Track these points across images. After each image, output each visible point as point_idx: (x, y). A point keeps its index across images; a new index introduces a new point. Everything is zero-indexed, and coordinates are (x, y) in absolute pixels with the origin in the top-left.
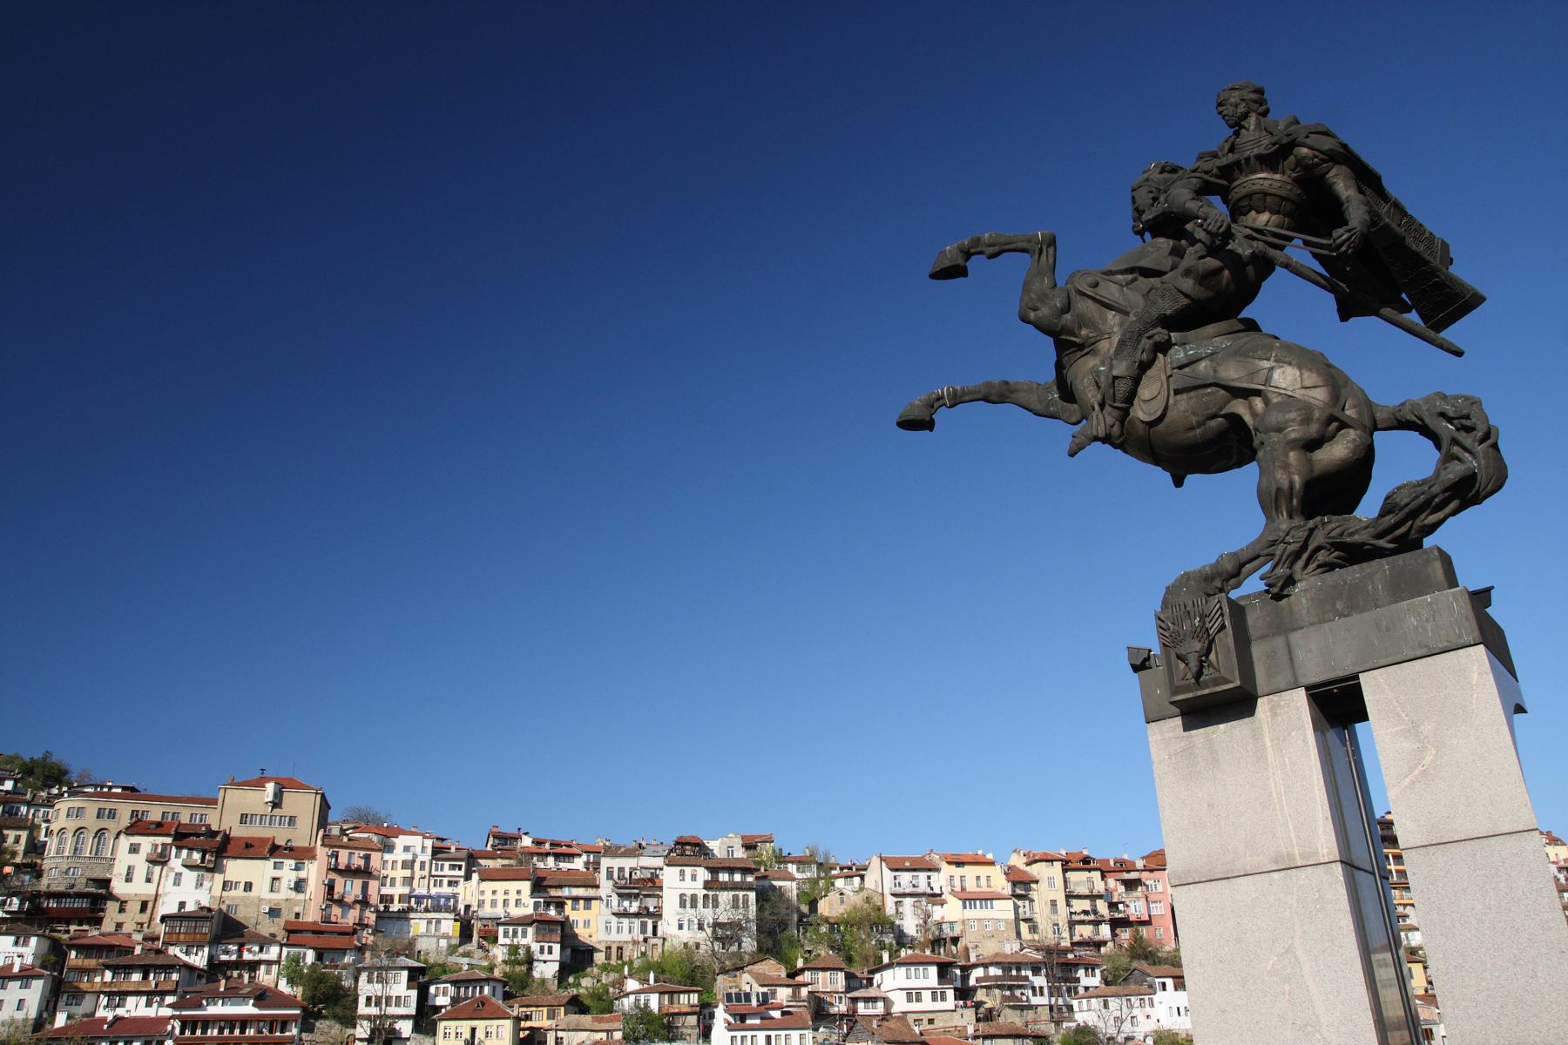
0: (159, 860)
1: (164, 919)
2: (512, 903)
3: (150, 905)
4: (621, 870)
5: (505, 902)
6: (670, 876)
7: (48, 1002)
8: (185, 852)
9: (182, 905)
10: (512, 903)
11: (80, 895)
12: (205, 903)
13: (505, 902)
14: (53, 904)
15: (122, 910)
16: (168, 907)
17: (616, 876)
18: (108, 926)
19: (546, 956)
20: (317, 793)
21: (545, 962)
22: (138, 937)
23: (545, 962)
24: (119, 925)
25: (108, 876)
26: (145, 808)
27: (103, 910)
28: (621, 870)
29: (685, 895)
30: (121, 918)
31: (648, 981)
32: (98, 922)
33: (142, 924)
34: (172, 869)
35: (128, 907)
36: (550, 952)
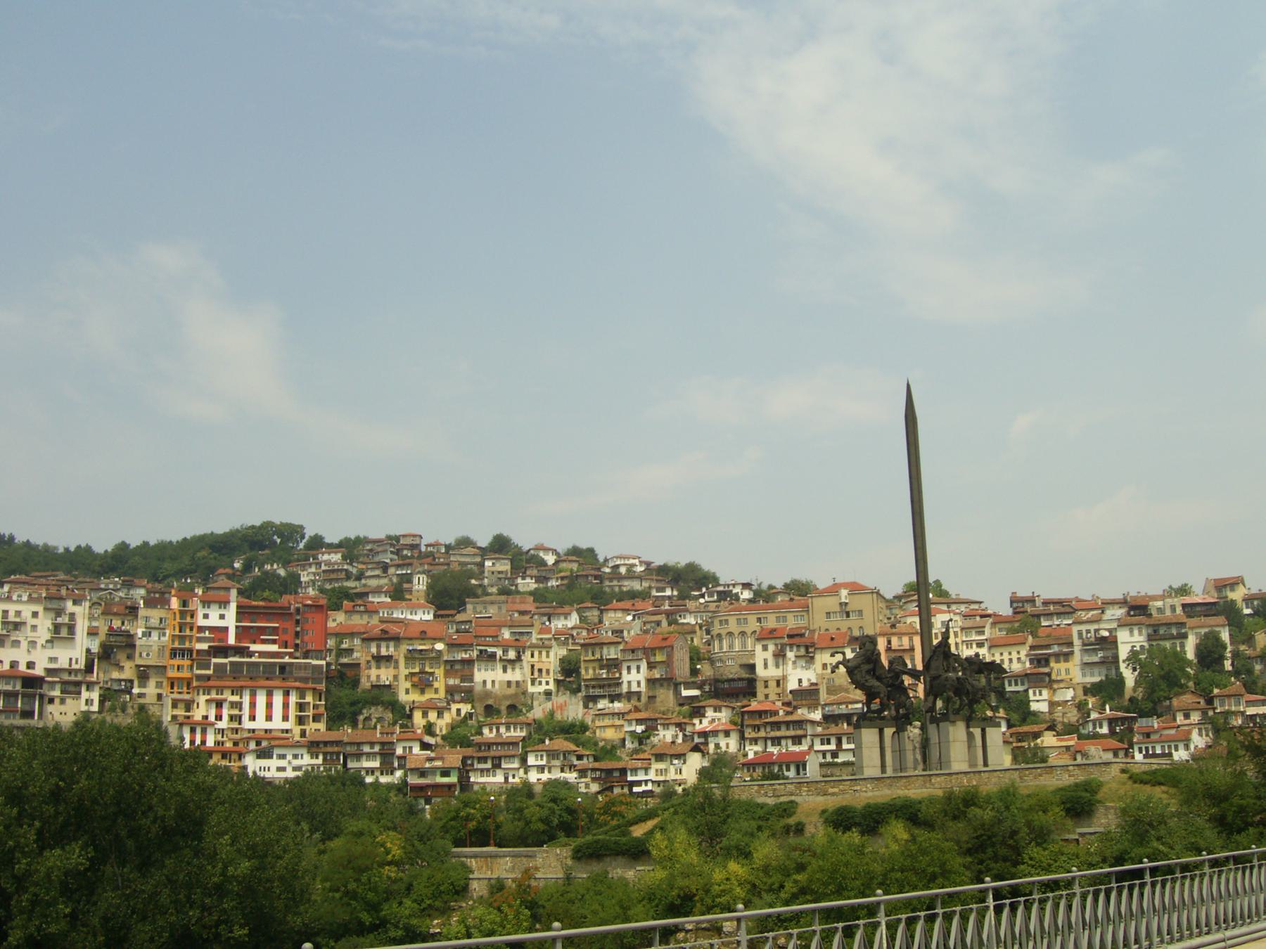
0: (780, 655)
1: (791, 692)
2: (1015, 661)
3: (781, 682)
4: (1088, 631)
5: (1011, 660)
6: (1123, 636)
7: (740, 744)
8: (795, 649)
9: (800, 681)
10: (1015, 661)
11: (740, 679)
12: (814, 681)
13: (1011, 660)
14: (726, 686)
15: (766, 687)
16: (792, 685)
17: (1084, 636)
18: (760, 696)
19: (1038, 697)
20: (872, 593)
21: (1038, 701)
22: (779, 704)
23: (1038, 701)
24: (767, 696)
25: (752, 662)
26: (765, 616)
27: (755, 688)
28: (1088, 631)
29: (1135, 646)
30: (766, 691)
31: (1105, 710)
32: (754, 695)
33: (779, 694)
34: (790, 659)
35: (769, 683)
36: (1040, 694)
